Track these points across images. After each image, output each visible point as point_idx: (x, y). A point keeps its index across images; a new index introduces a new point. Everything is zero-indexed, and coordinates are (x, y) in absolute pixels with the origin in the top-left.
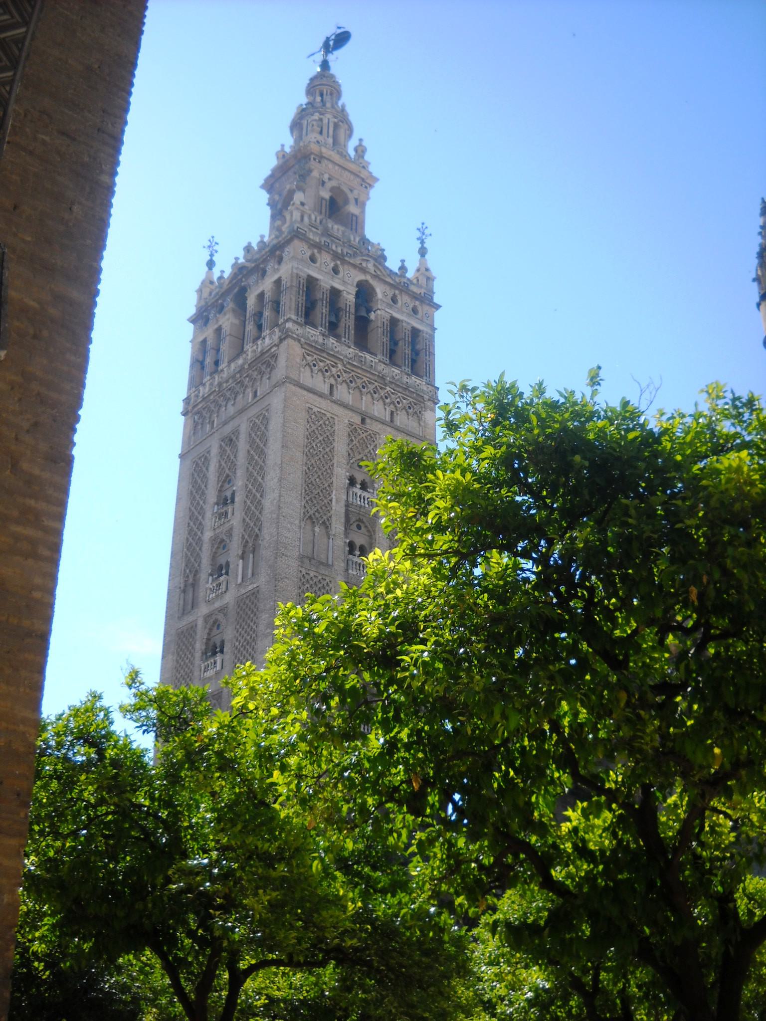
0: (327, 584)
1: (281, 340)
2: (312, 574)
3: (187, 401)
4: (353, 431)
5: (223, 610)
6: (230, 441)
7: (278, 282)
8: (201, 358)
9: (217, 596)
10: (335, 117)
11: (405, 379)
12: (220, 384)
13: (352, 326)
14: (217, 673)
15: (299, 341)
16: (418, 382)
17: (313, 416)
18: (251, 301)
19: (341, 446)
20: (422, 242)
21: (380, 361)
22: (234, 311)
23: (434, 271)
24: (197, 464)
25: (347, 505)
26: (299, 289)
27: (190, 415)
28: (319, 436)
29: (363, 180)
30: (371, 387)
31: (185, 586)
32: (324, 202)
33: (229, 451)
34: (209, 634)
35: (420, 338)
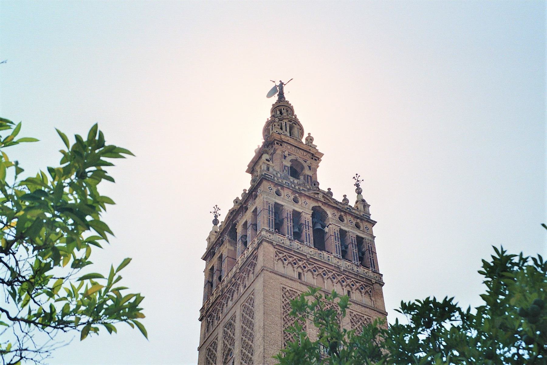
3: (202, 310)
6: (230, 325)
7: (255, 211)
8: (210, 280)
10: (290, 121)
11: (355, 269)
16: (366, 271)
17: (287, 293)
18: (239, 230)
21: (335, 257)
22: (229, 241)
23: (368, 202)
24: (209, 350)
26: (269, 211)
27: (205, 318)
30: (330, 275)
33: (229, 332)
35: (364, 243)
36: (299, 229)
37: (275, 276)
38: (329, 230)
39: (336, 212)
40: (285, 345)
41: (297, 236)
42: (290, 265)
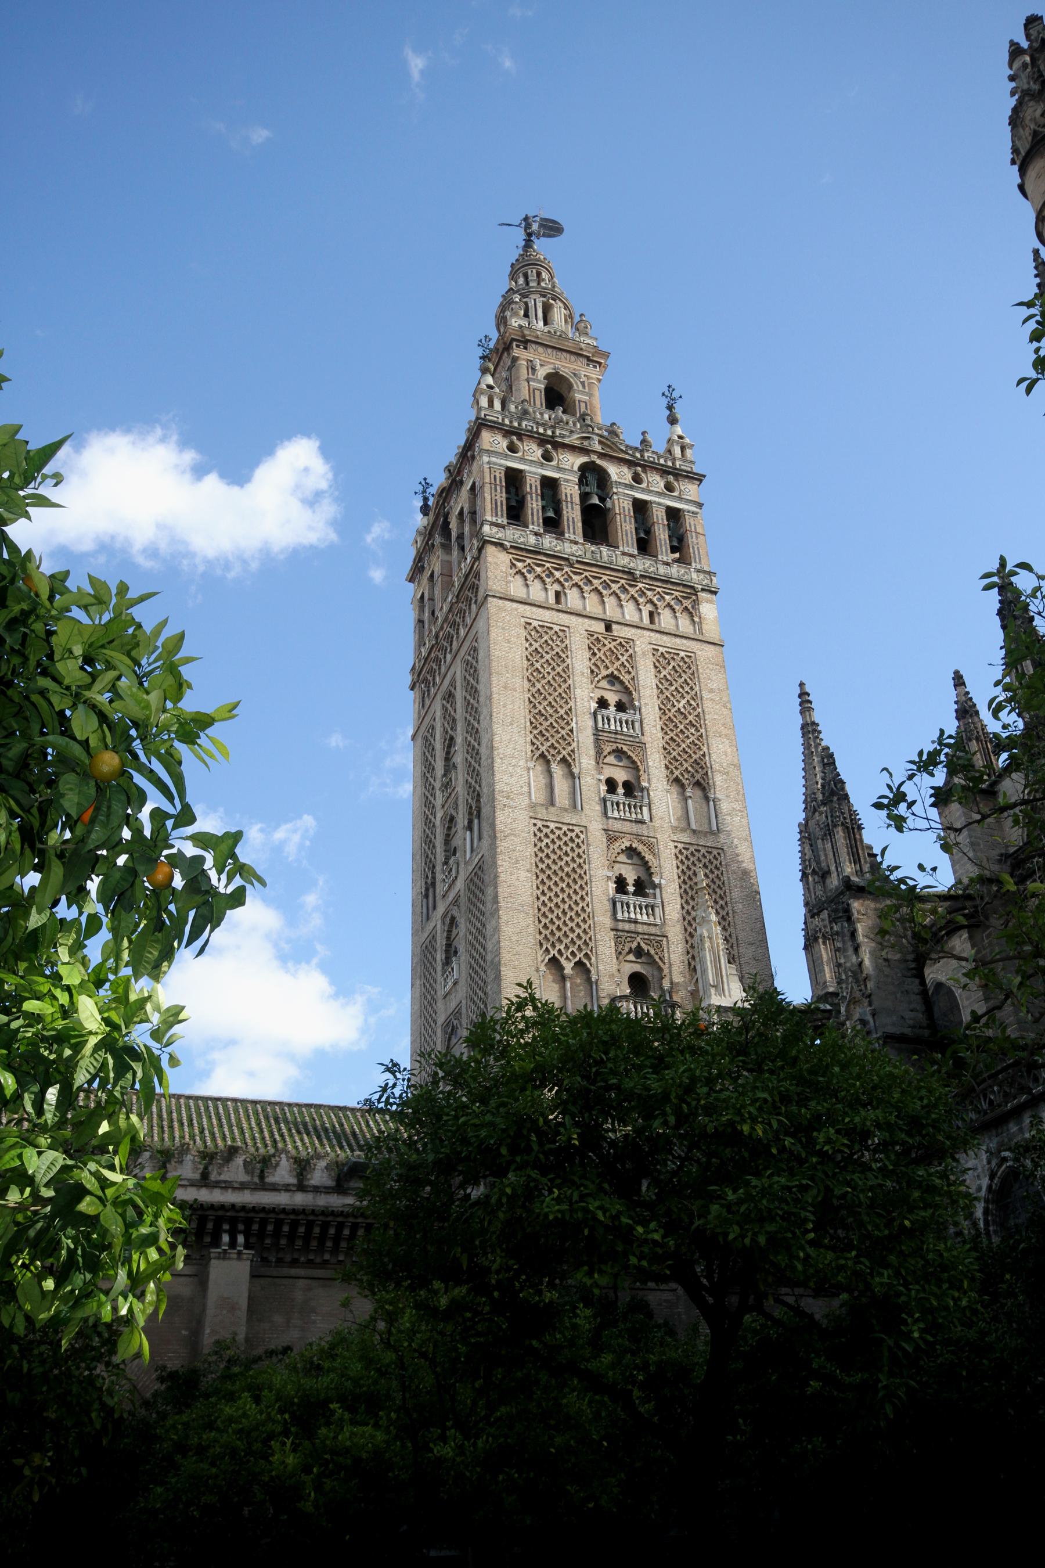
0: (577, 836)
2: (552, 826)
4: (594, 642)
5: (455, 902)
6: (450, 696)
7: (473, 488)
9: (450, 887)
10: (544, 296)
12: (437, 636)
13: (579, 518)
14: (455, 983)
15: (502, 545)
18: (453, 525)
19: (580, 662)
20: (670, 408)
21: (623, 554)
26: (496, 485)
28: (546, 653)
29: (588, 358)
31: (427, 889)
32: (537, 393)
34: (448, 938)
36: (555, 514)
37: (510, 604)
38: (613, 503)
39: (625, 470)
40: (532, 723)
41: (553, 524)
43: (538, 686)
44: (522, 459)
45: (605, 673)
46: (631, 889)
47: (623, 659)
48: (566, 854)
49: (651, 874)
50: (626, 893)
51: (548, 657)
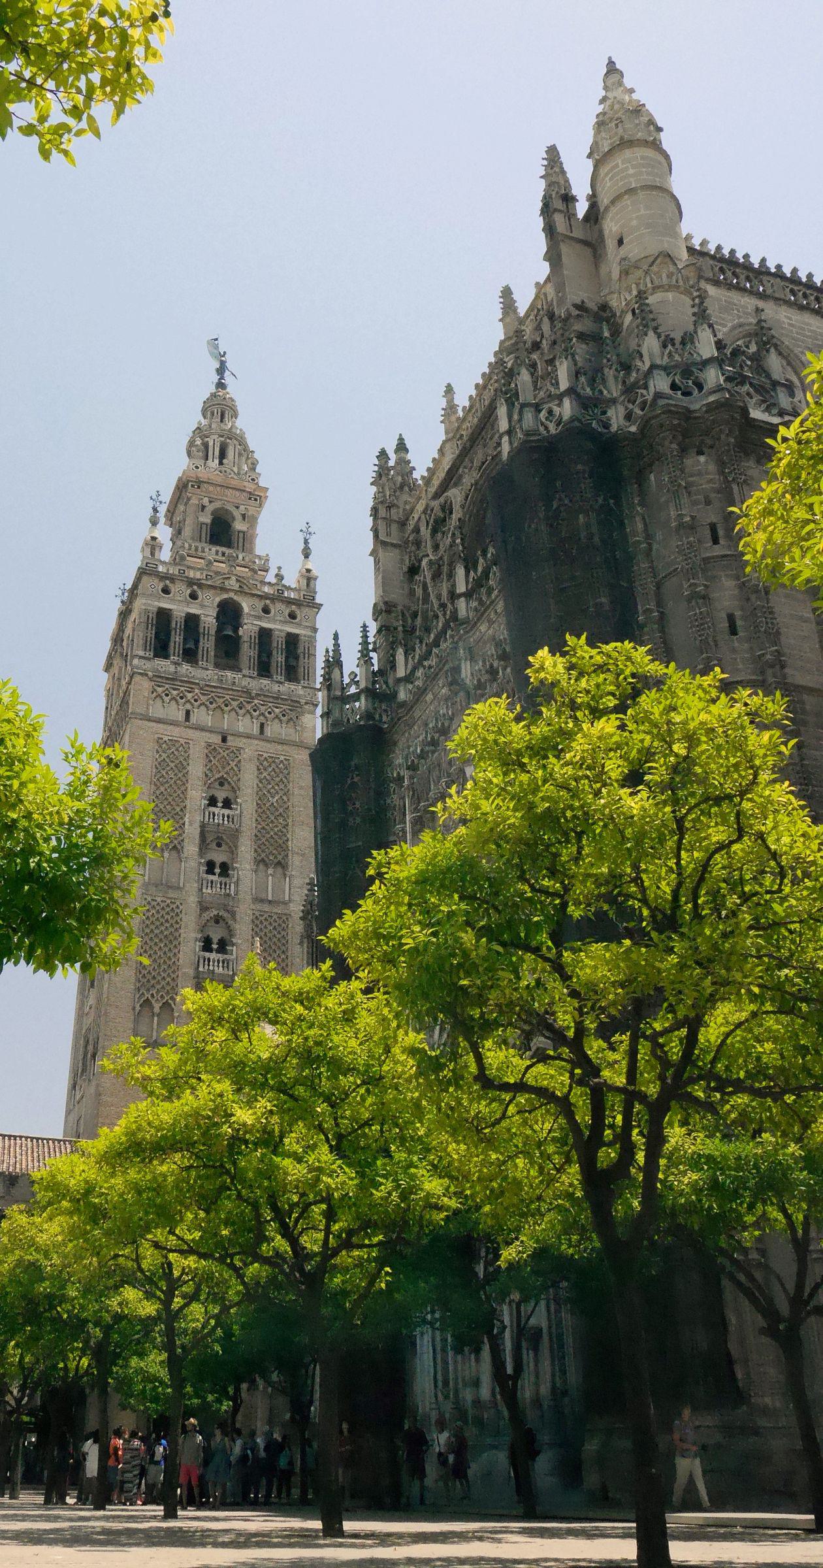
0: (178, 907)
1: (131, 677)
2: (159, 899)
4: (211, 750)
11: (276, 687)
18: (125, 644)
19: (196, 769)
20: (306, 542)
23: (315, 572)
25: (203, 826)
29: (250, 493)
30: (235, 704)
32: (204, 527)
42: (173, 702)
43: (162, 789)
44: (173, 600)
45: (217, 776)
46: (215, 946)
47: (233, 764)
48: (167, 921)
49: (231, 936)
50: (210, 950)
51: (172, 765)
